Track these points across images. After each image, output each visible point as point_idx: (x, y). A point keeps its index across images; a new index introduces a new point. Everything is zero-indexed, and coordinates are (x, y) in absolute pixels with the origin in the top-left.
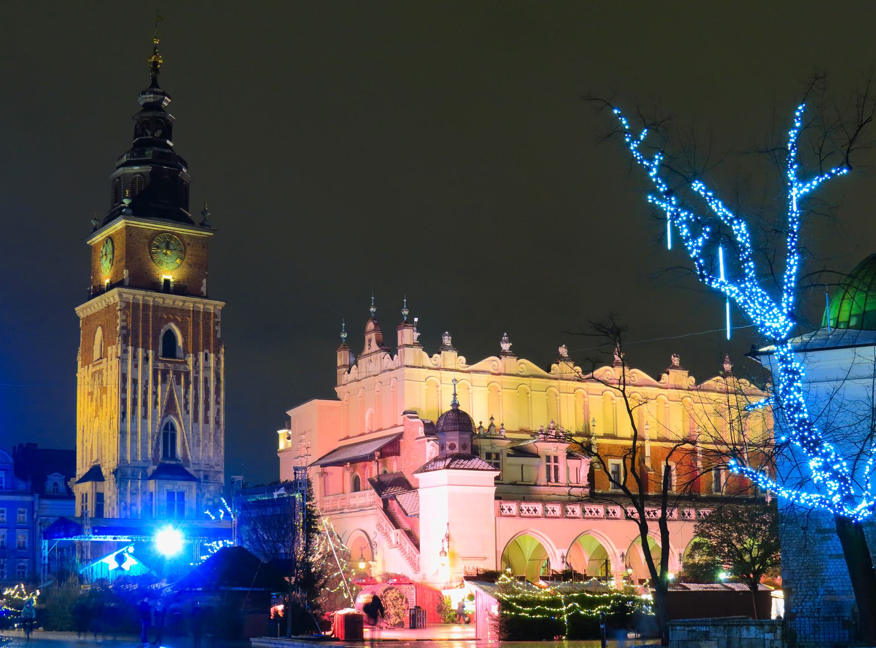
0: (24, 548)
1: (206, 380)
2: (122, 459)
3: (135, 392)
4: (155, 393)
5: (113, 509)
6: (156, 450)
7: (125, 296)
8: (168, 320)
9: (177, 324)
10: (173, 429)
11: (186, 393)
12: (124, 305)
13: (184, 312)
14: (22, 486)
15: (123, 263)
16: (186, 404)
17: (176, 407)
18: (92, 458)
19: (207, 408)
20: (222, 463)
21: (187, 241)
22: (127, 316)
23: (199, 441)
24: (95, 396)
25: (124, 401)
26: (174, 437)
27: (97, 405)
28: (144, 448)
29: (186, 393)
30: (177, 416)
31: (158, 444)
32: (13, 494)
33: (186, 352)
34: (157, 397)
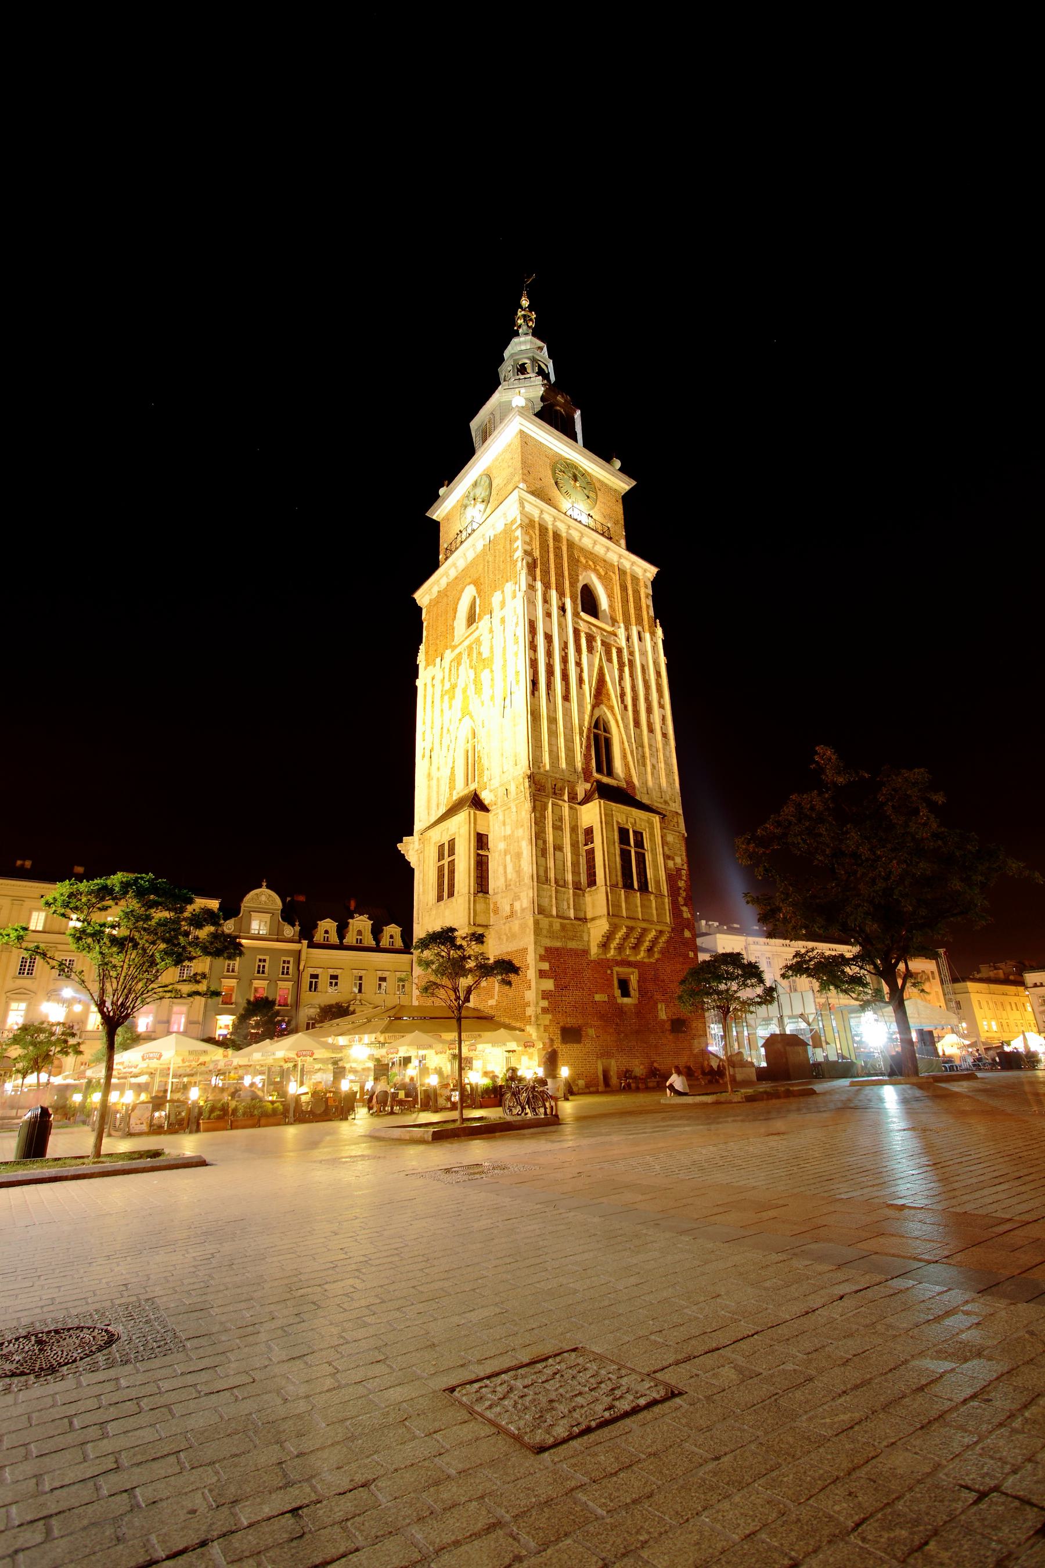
0: (286, 1005)
1: (644, 669)
2: (536, 760)
3: (549, 654)
4: (578, 664)
5: (518, 855)
6: (587, 757)
7: (526, 504)
8: (586, 567)
9: (600, 577)
10: (607, 730)
11: (621, 678)
12: (527, 521)
13: (607, 565)
14: (289, 931)
15: (517, 478)
16: (623, 695)
17: (609, 695)
18: (452, 788)
19: (649, 710)
20: (679, 799)
21: (597, 485)
22: (531, 537)
23: (643, 757)
24: (458, 691)
25: (534, 664)
26: (608, 743)
27: (465, 698)
28: (570, 750)
29: (621, 678)
30: (611, 708)
31: (588, 747)
32: (278, 941)
33: (614, 621)
34: (582, 671)
